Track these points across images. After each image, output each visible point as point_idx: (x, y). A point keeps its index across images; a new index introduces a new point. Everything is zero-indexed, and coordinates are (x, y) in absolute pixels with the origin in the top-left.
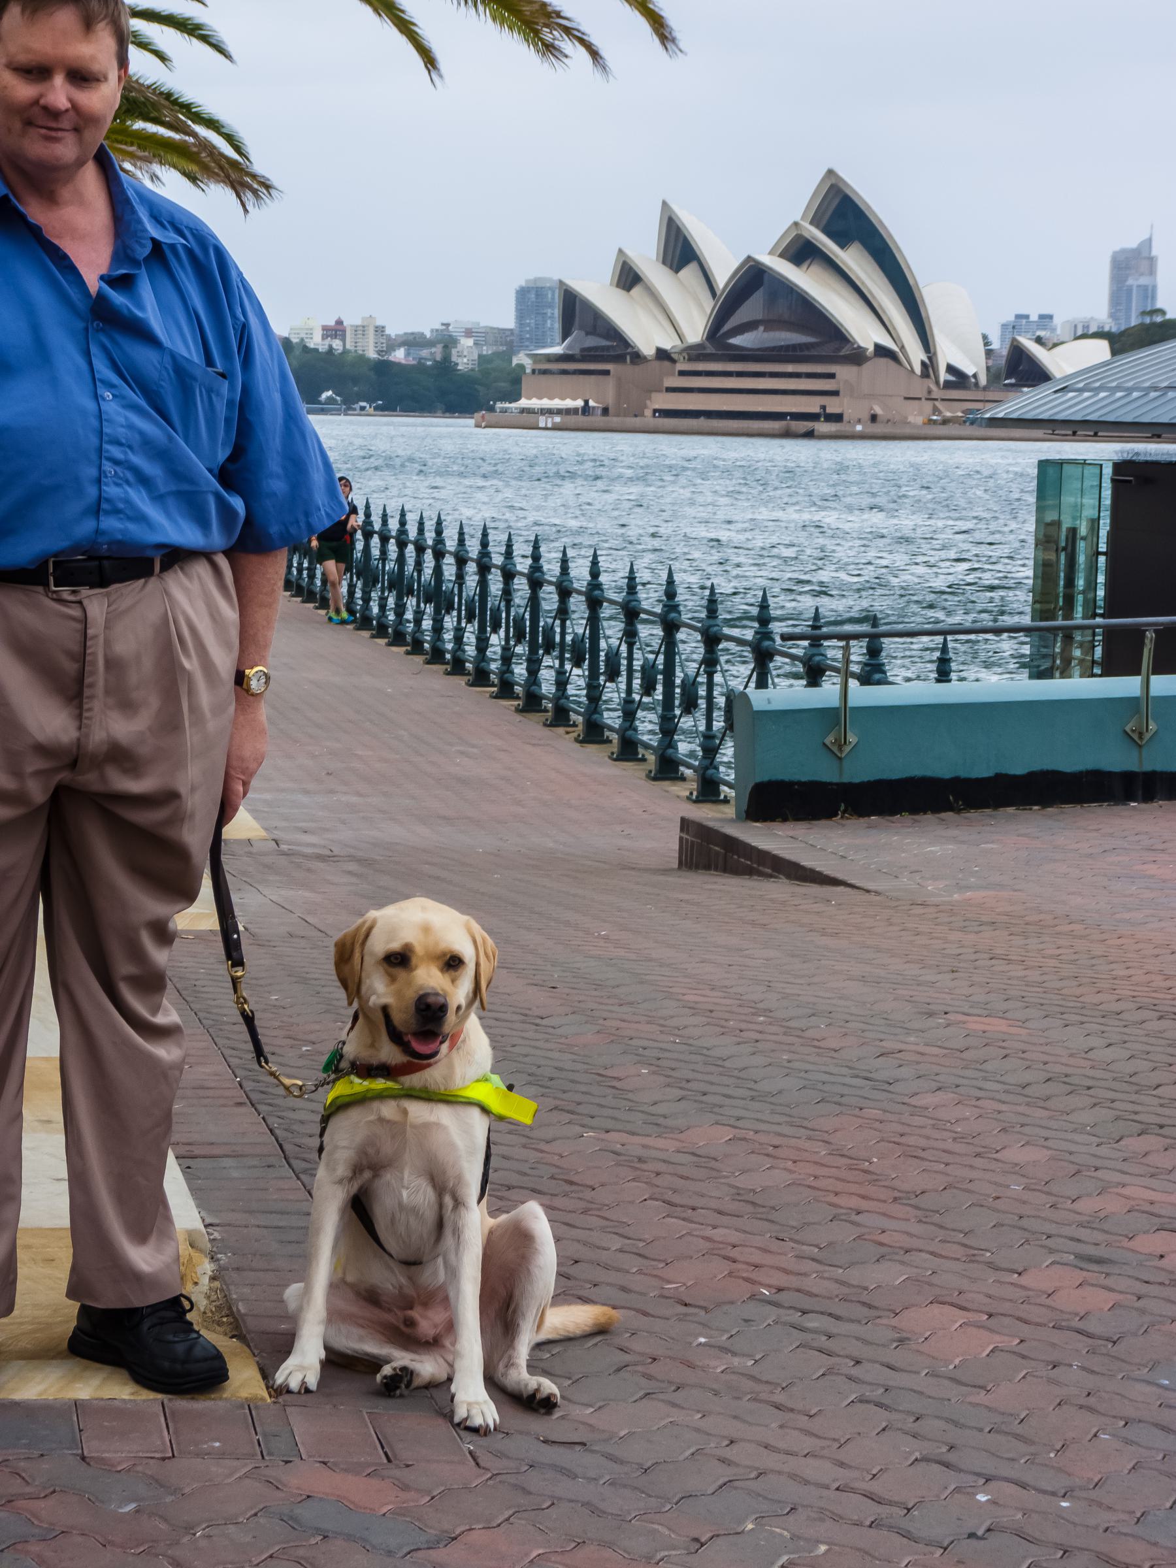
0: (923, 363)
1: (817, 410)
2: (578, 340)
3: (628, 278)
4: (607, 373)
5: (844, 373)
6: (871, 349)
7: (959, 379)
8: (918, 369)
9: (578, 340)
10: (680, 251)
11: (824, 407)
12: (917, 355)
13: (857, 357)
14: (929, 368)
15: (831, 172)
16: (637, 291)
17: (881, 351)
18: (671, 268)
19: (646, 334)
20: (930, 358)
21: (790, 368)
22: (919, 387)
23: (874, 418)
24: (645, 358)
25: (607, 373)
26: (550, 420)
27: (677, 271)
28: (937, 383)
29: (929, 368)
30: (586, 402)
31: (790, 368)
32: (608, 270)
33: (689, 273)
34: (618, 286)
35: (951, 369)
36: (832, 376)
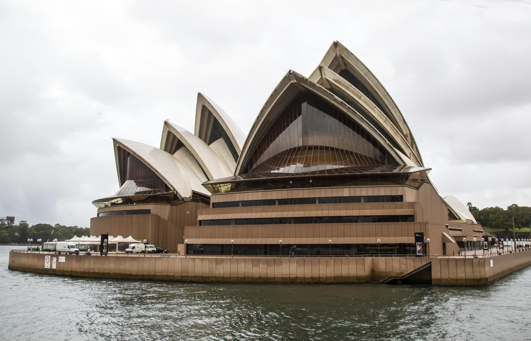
2: (132, 188)
3: (173, 143)
4: (148, 212)
9: (132, 188)
10: (212, 127)
15: (336, 44)
16: (178, 154)
18: (205, 141)
19: (183, 180)
21: (346, 192)
24: (183, 199)
27: (209, 144)
30: (105, 237)
32: (156, 140)
33: (219, 145)
34: (165, 150)
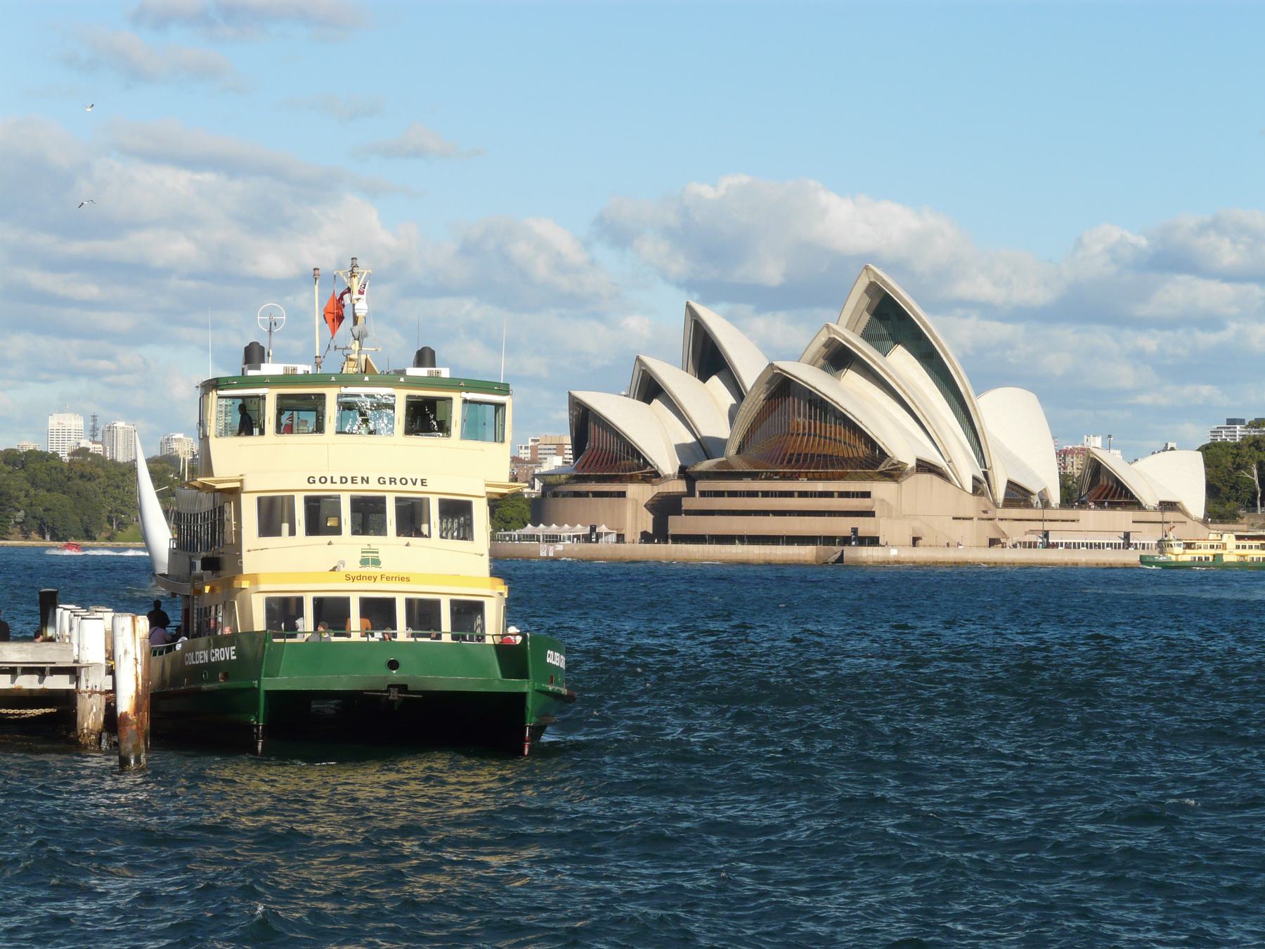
0: (975, 478)
1: (848, 533)
5: (881, 490)
6: (912, 464)
7: (1018, 495)
8: (969, 487)
11: (855, 531)
12: (966, 469)
13: (895, 473)
17: (924, 467)
20: (985, 474)
21: (820, 486)
22: (970, 505)
25: (622, 494)
26: (551, 548)
28: (996, 504)
29: (980, 486)
30: (593, 529)
31: (820, 486)
35: (1011, 485)
36: (866, 495)
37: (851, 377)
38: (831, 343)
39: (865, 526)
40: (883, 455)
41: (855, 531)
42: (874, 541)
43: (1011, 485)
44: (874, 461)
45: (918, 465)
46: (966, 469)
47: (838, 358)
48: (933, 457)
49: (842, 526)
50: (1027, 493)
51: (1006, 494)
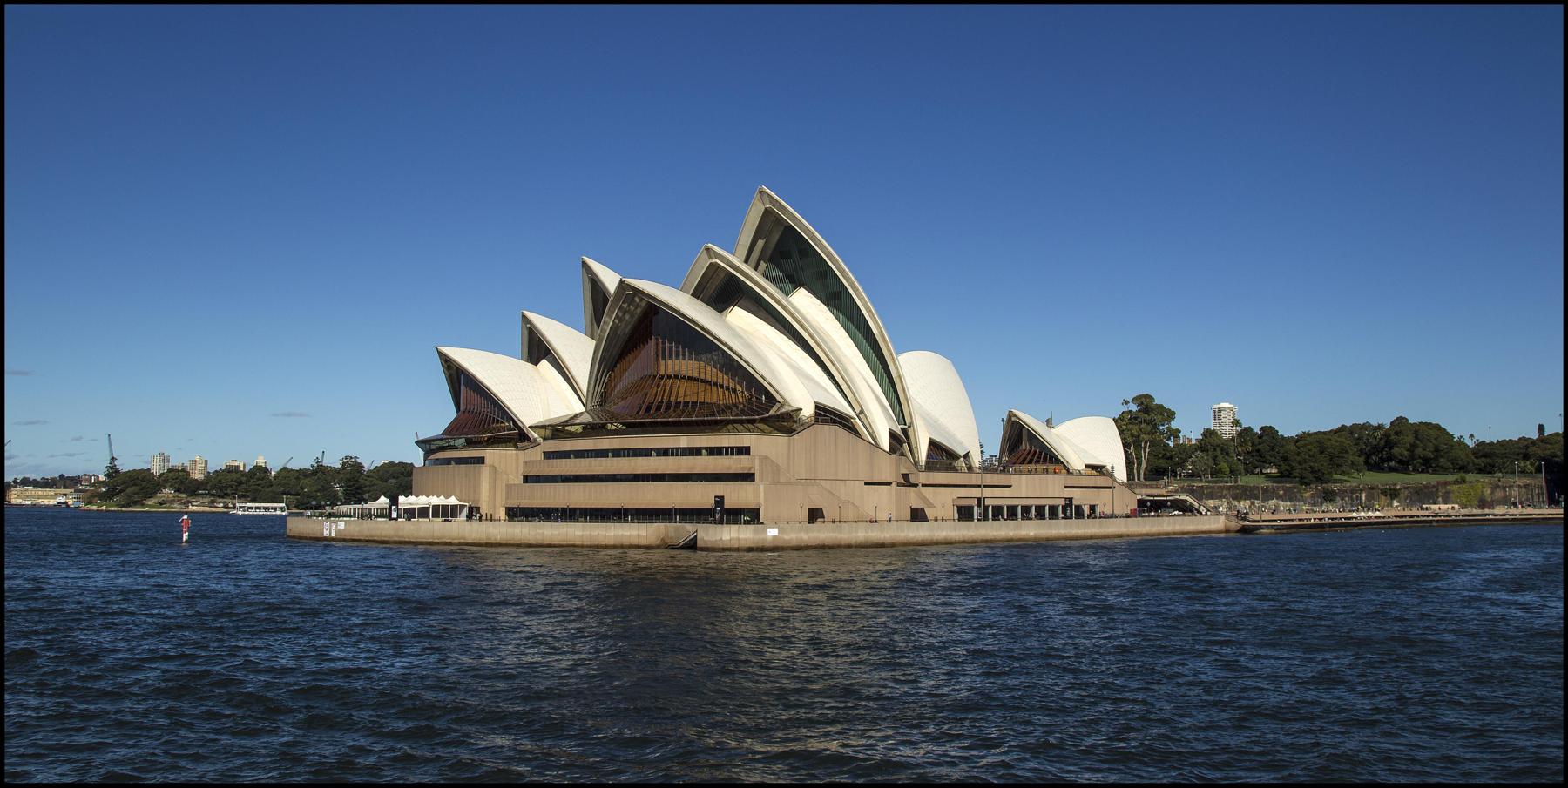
0: (892, 435)
4: (481, 461)
5: (765, 444)
6: (808, 411)
7: (942, 456)
8: (885, 443)
11: (720, 501)
12: (882, 424)
13: (786, 423)
14: (900, 441)
16: (544, 363)
17: (824, 414)
20: (904, 431)
21: (684, 441)
22: (887, 468)
23: (815, 515)
25: (481, 461)
29: (900, 441)
36: (745, 451)
37: (739, 317)
38: (713, 268)
39: (736, 495)
40: (772, 400)
41: (720, 501)
42: (753, 516)
43: (933, 445)
44: (759, 407)
45: (817, 414)
46: (882, 424)
47: (723, 291)
48: (838, 403)
49: (700, 495)
50: (953, 456)
51: (928, 456)
